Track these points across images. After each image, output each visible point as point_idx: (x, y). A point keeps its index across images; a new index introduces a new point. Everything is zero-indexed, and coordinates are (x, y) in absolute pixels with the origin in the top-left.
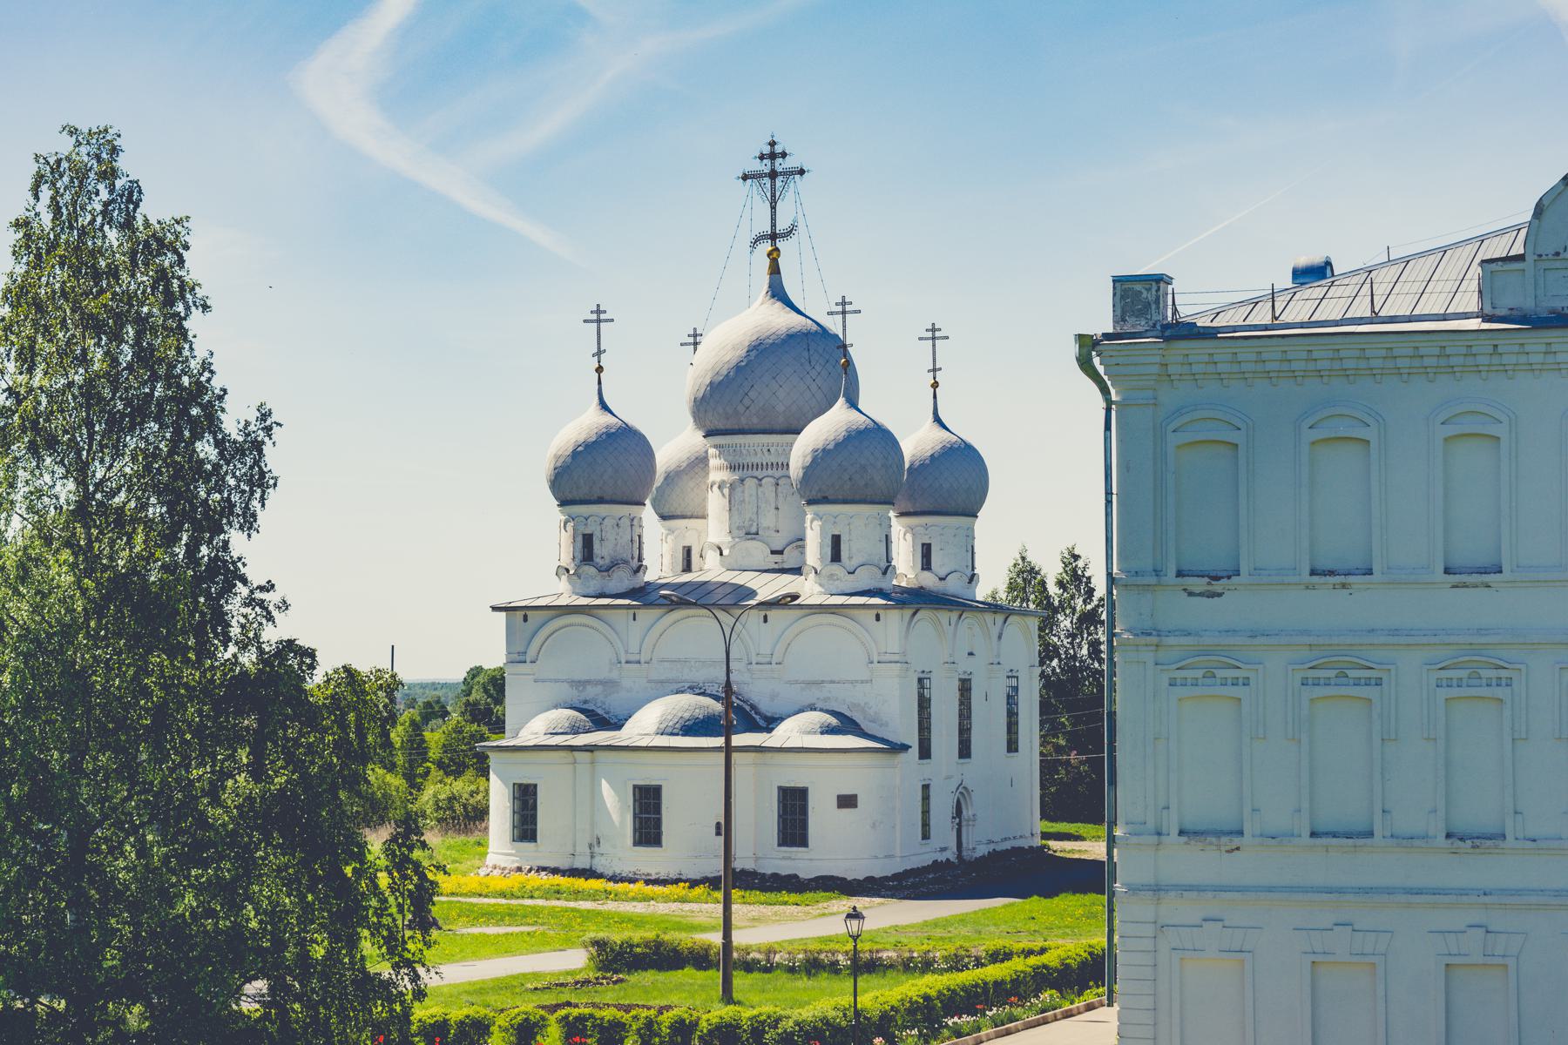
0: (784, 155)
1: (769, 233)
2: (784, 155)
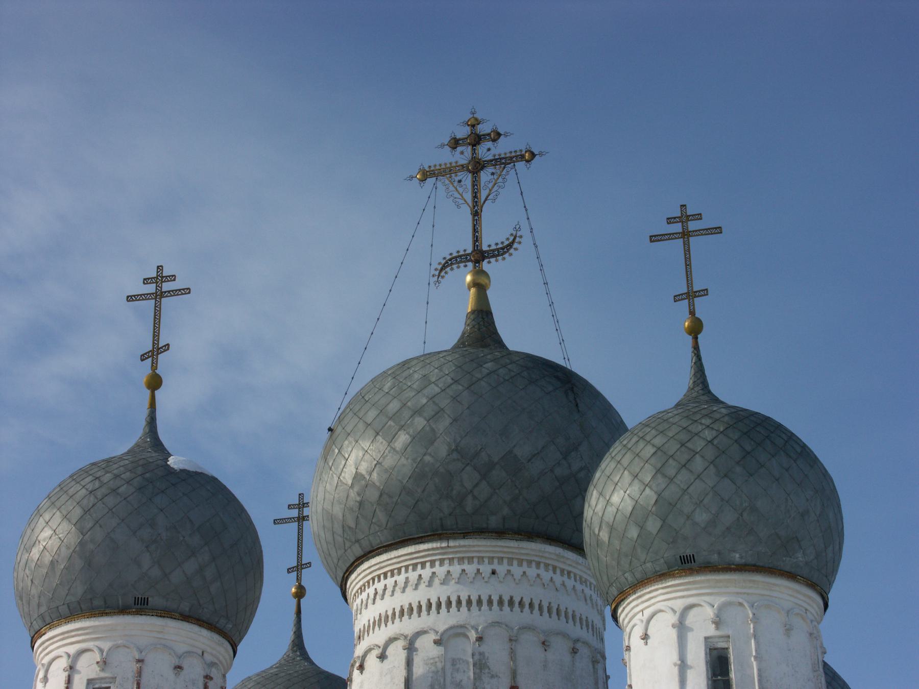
0: (496, 136)
1: (470, 250)
2: (496, 136)
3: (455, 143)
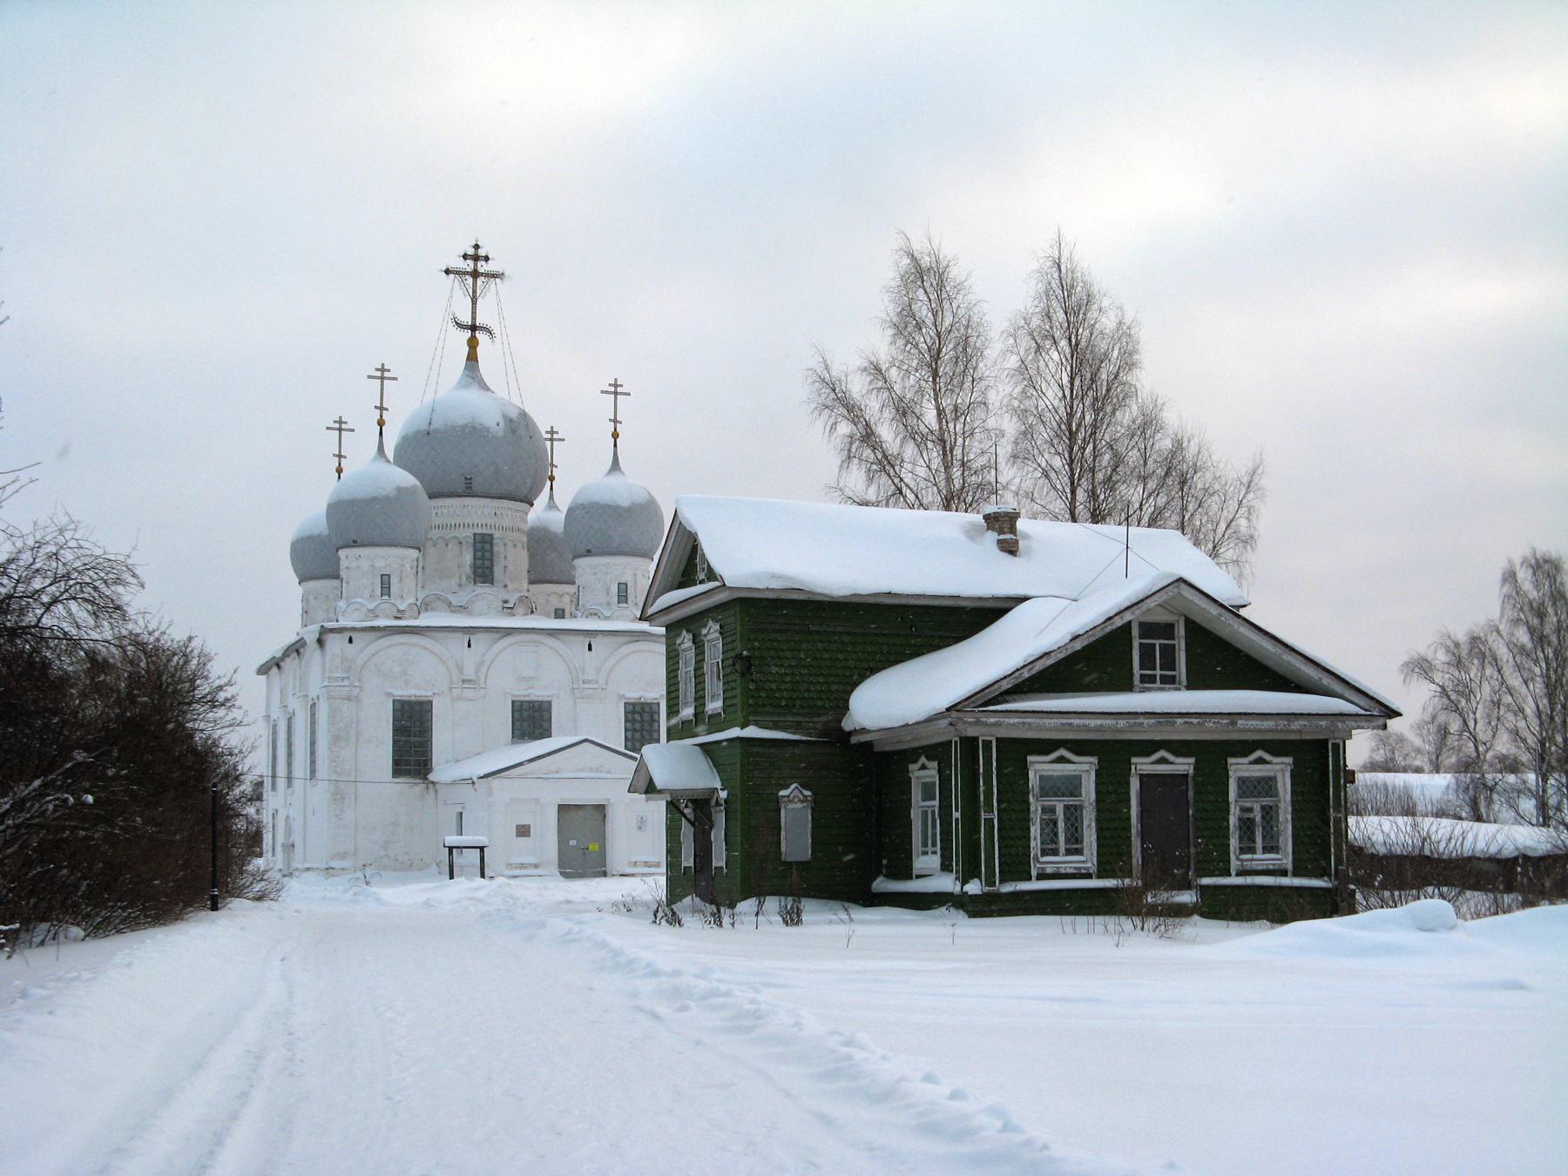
0: (487, 259)
2: (487, 259)
3: (465, 257)
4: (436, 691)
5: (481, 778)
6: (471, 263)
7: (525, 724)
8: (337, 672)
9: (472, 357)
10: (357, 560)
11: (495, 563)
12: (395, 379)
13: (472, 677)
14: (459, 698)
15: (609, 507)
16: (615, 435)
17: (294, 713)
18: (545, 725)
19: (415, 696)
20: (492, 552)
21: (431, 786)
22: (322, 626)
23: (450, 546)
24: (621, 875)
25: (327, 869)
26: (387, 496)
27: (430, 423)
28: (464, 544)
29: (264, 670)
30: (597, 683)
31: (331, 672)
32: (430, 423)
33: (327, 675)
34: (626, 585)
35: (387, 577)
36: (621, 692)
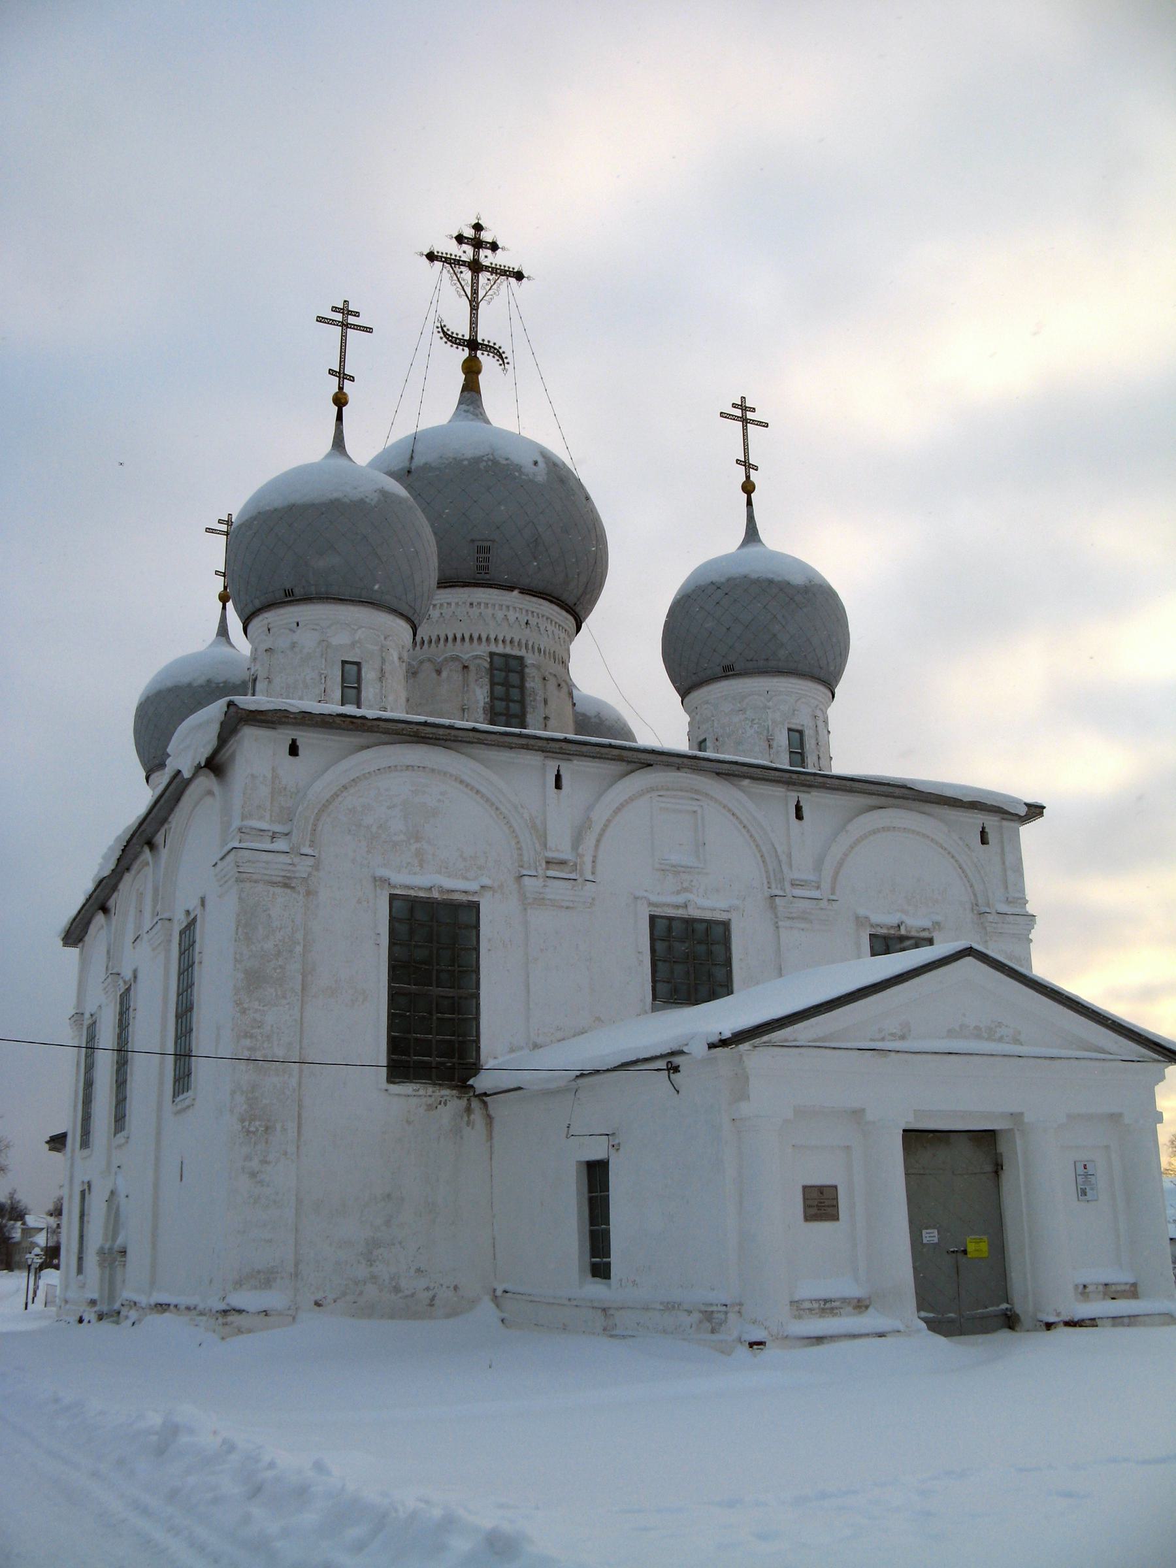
0: (494, 247)
1: (467, 337)
3: (460, 239)
4: (486, 881)
5: (724, 1043)
6: (469, 250)
7: (679, 969)
8: (261, 818)
9: (471, 387)
10: (291, 630)
11: (529, 709)
12: (368, 330)
13: (566, 854)
14: (540, 901)
15: (771, 582)
16: (748, 488)
17: (135, 977)
18: (719, 973)
19: (442, 890)
20: (522, 688)
21: (475, 1104)
22: (230, 704)
23: (444, 674)
24: (1070, 1324)
25: (225, 1312)
26: (362, 501)
27: (412, 457)
28: (472, 668)
29: (75, 934)
30: (818, 888)
31: (243, 818)
32: (412, 457)
33: (237, 823)
34: (801, 732)
35: (355, 668)
36: (862, 912)
